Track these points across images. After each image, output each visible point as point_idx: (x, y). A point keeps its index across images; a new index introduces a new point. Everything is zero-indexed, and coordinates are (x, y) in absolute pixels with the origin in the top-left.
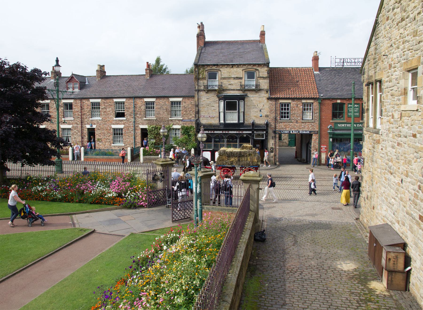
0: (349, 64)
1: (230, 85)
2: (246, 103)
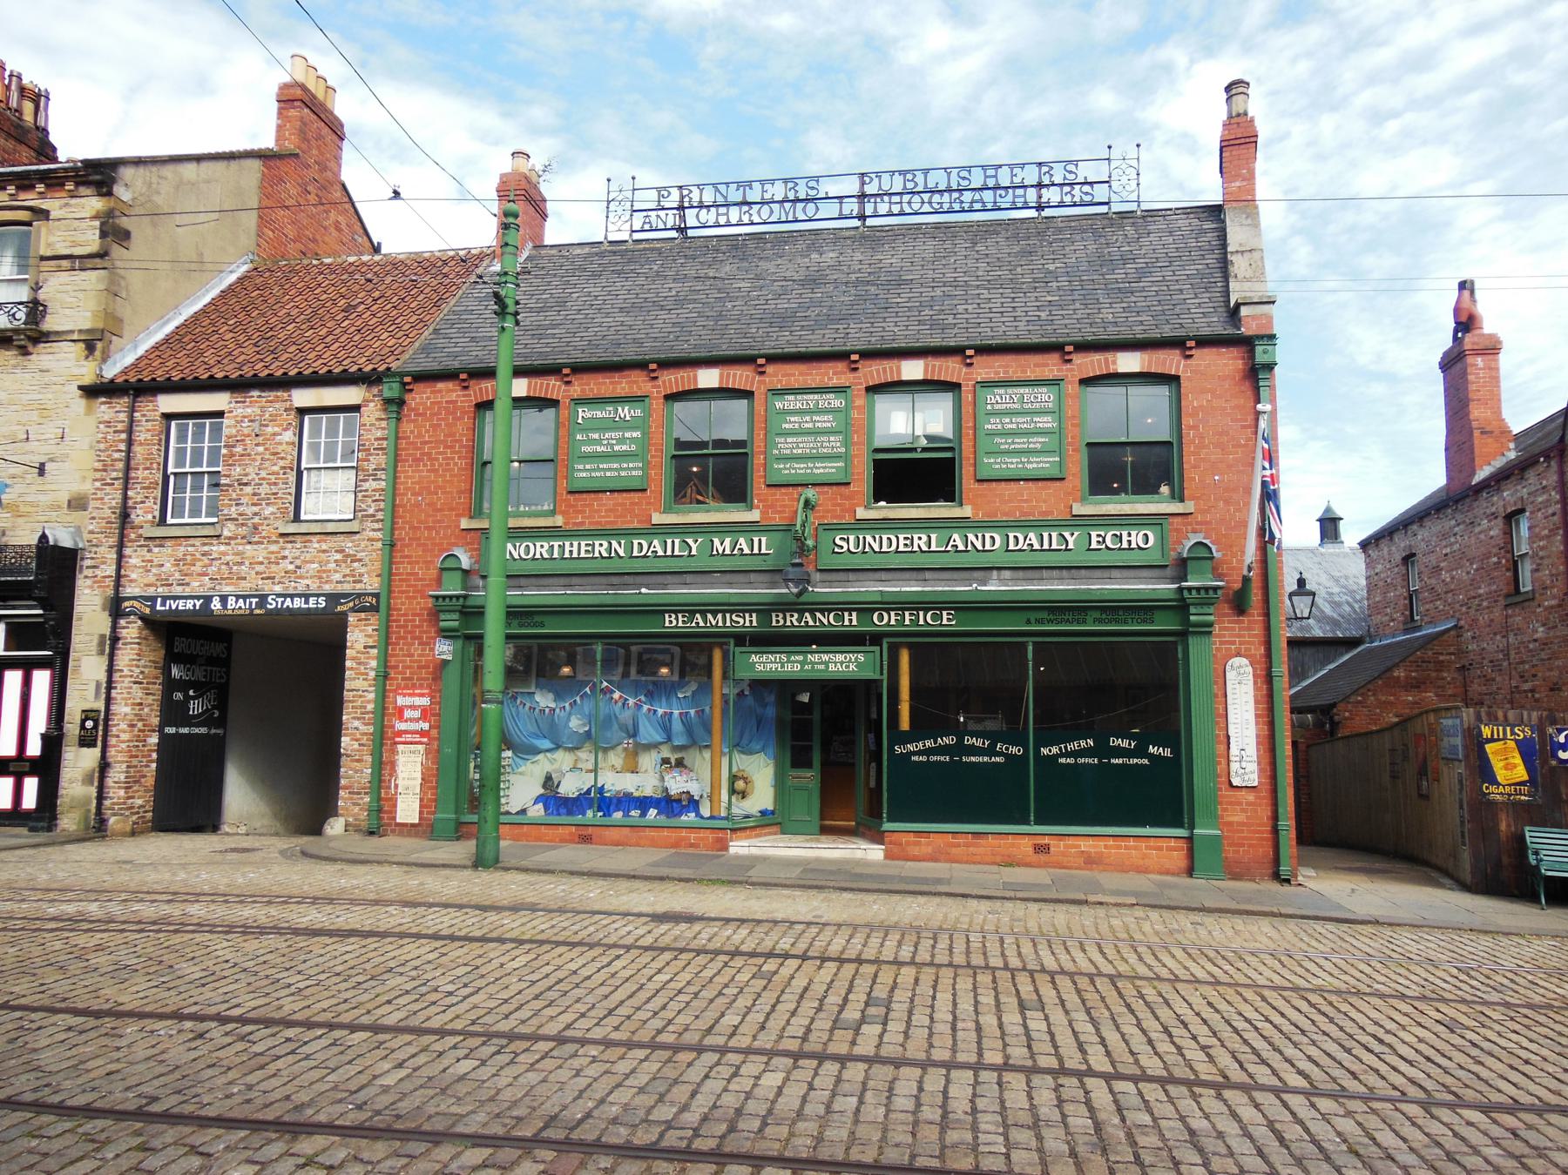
0: (709, 216)
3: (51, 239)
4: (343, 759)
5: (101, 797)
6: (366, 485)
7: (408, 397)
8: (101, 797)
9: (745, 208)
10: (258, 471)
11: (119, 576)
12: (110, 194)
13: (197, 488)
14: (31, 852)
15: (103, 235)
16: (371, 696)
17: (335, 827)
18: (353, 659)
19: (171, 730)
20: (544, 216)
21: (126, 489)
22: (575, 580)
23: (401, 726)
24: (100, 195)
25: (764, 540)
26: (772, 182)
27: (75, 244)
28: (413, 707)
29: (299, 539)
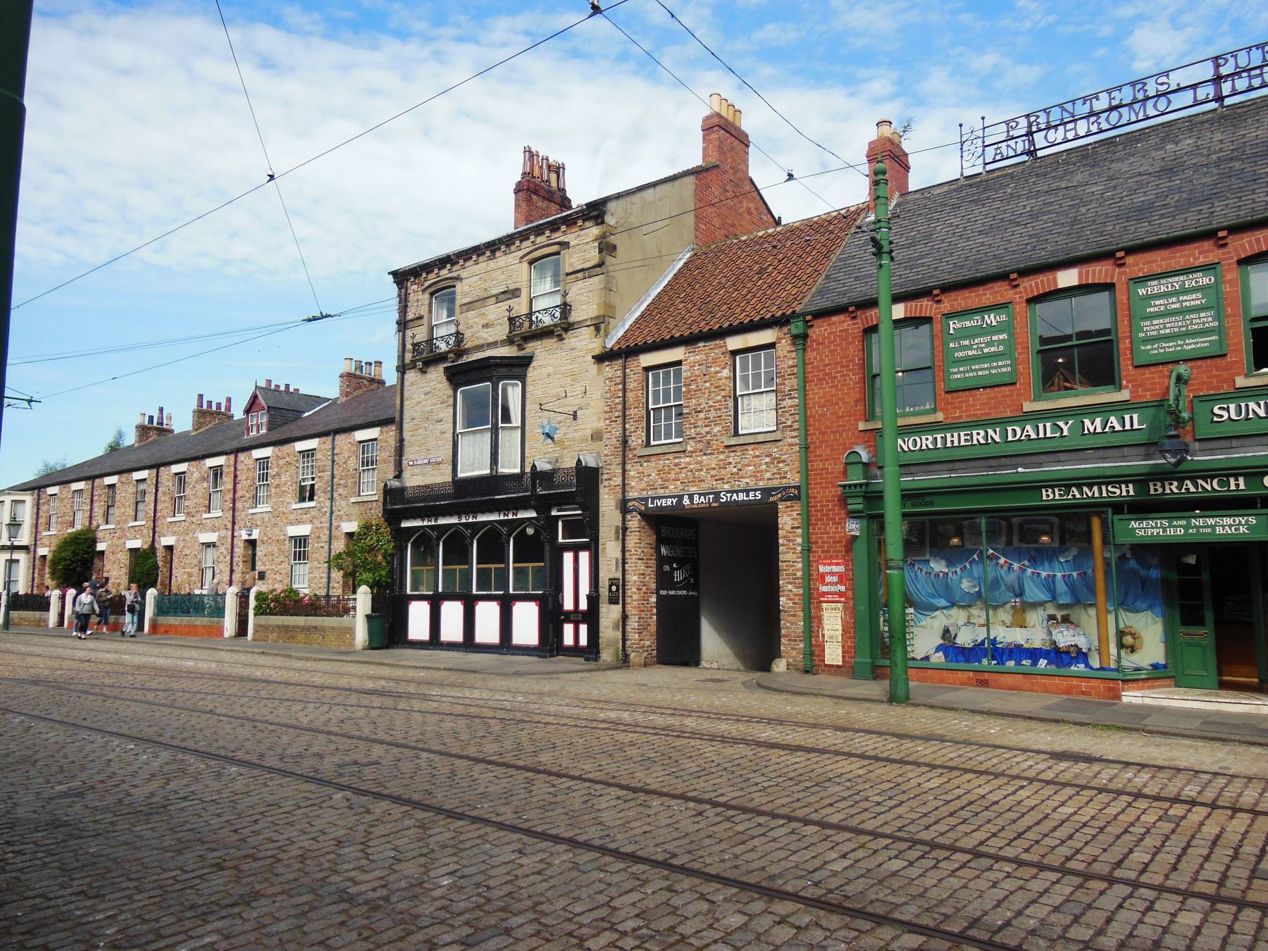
0: (1058, 135)
1: (486, 326)
2: (529, 388)
3: (572, 260)
4: (782, 615)
5: (624, 639)
6: (784, 403)
7: (810, 331)
8: (624, 639)
9: (1093, 119)
10: (706, 401)
11: (624, 484)
12: (603, 222)
13: (668, 418)
14: (587, 674)
15: (601, 251)
16: (800, 565)
17: (780, 666)
18: (784, 537)
19: (663, 592)
20: (906, 168)
21: (624, 423)
22: (957, 465)
23: (824, 589)
24: (597, 224)
25: (1135, 416)
26: (1119, 88)
27: (585, 261)
28: (832, 574)
29: (738, 448)
